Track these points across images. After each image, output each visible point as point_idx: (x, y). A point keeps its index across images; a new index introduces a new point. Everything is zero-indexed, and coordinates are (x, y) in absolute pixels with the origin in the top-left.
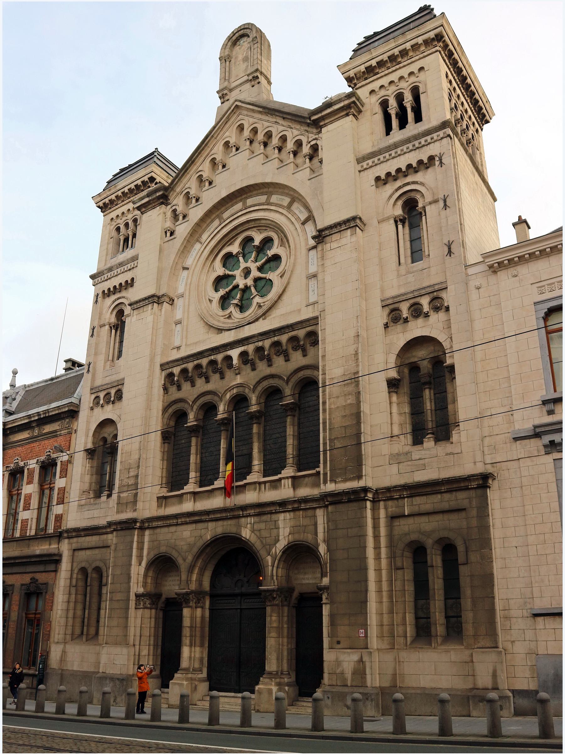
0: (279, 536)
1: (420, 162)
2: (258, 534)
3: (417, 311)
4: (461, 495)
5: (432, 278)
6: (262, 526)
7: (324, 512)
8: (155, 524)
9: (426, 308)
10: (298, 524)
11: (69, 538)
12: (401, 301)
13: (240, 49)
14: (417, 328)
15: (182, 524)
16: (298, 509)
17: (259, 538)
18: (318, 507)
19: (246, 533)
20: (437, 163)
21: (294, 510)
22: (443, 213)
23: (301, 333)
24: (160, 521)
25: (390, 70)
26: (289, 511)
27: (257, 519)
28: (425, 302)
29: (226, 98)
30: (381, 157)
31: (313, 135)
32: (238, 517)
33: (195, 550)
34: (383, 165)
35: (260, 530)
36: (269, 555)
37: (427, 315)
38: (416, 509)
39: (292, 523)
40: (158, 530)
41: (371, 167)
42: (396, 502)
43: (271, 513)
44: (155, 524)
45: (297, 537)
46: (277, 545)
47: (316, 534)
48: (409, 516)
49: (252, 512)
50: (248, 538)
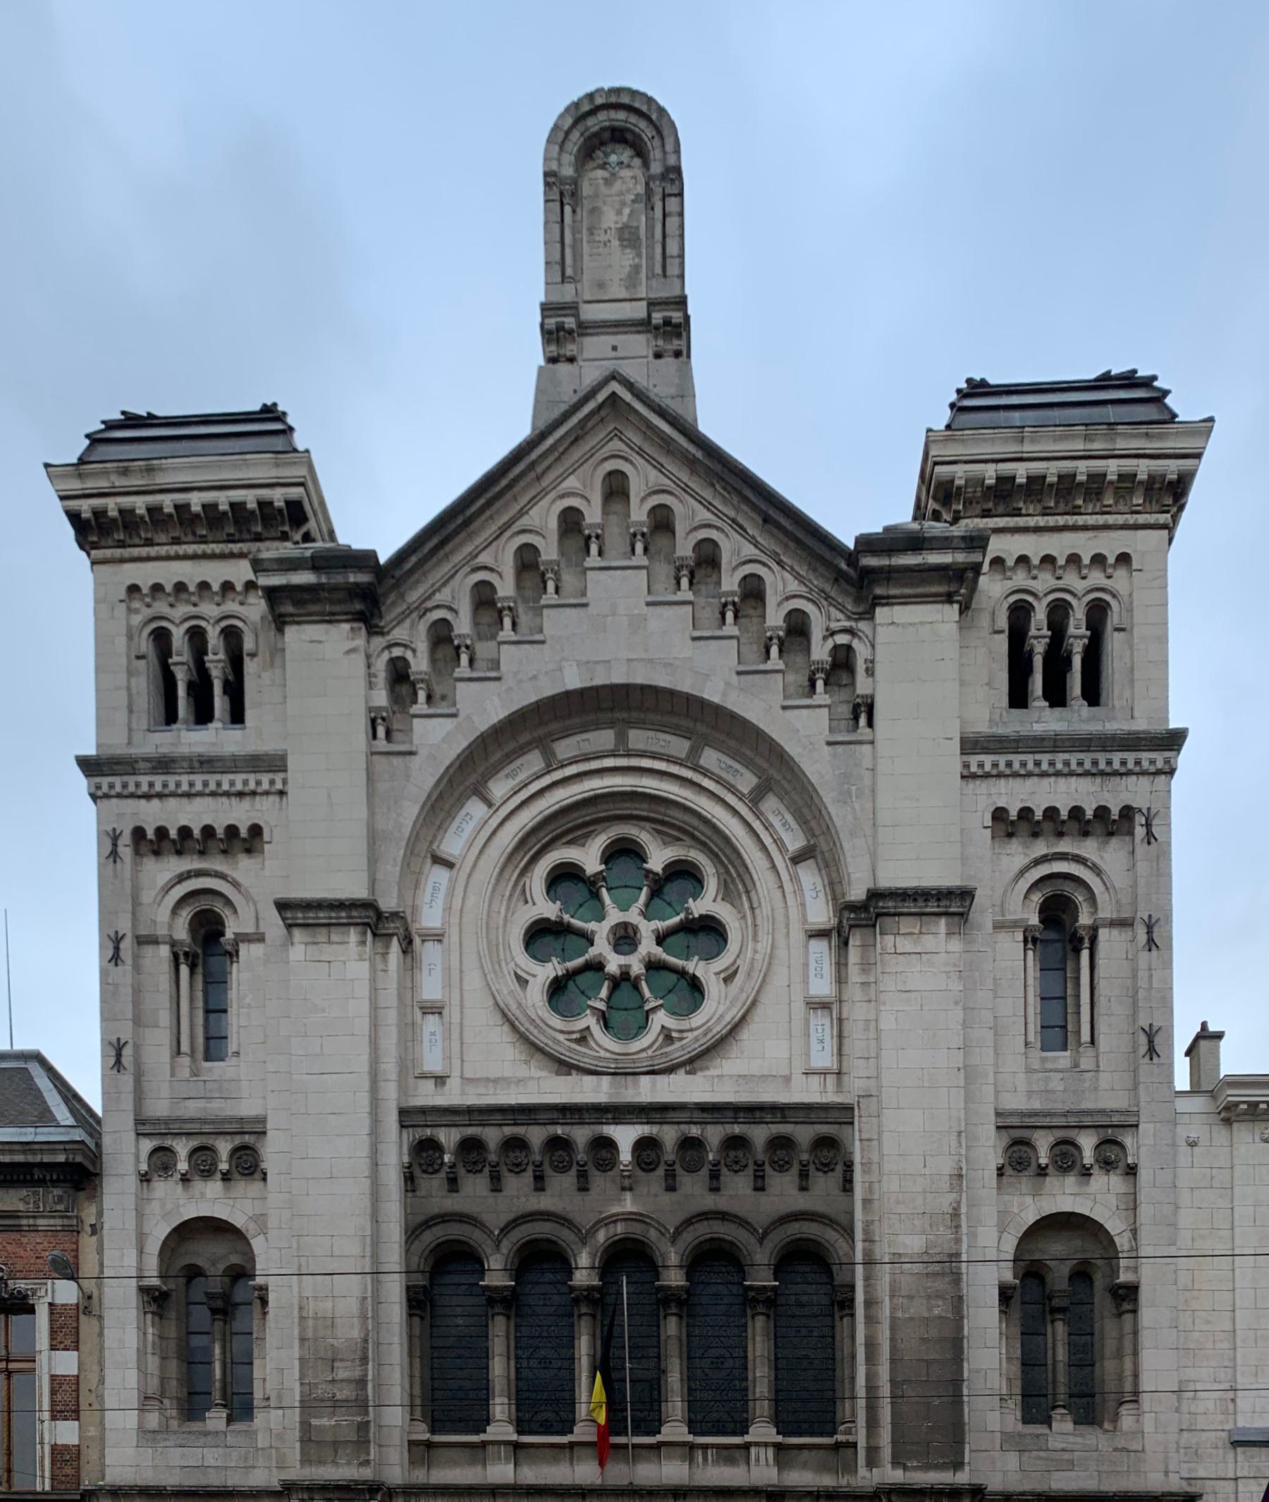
1: (1102, 812)
3: (1066, 1159)
5: (1107, 1094)
9: (1088, 1157)
12: (1036, 1127)
13: (608, 182)
14: (1064, 1196)
20: (1140, 832)
22: (1144, 955)
23: (804, 1134)
25: (1052, 521)
28: (1088, 1143)
29: (570, 349)
30: (1016, 759)
31: (841, 616)
34: (1015, 784)
37: (1086, 1173)
41: (987, 776)
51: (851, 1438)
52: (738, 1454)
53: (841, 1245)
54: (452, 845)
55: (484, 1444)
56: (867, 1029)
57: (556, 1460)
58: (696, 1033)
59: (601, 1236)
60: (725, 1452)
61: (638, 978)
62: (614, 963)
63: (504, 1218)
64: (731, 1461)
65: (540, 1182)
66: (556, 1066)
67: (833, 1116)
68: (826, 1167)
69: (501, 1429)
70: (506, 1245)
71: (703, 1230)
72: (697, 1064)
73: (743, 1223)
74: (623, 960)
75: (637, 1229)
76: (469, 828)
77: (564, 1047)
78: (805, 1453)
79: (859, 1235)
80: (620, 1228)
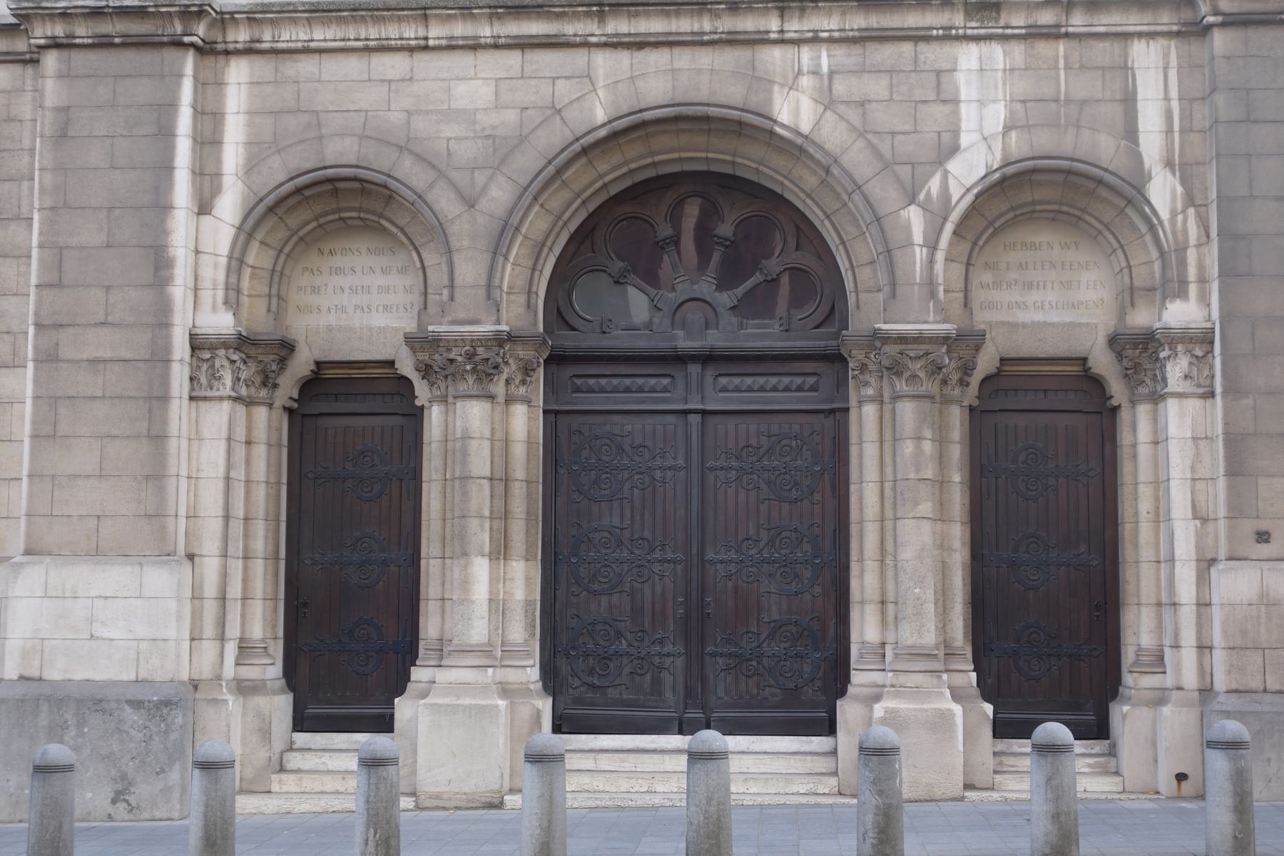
0: (956, 133)
2: (855, 117)
6: (876, 87)
7: (1166, 55)
15: (451, 47)
18: (1140, 35)
19: (794, 110)
24: (326, 22)
26: (1004, 38)
27: (843, 55)
33: (528, 162)
36: (912, 200)
39: (1022, 86)
40: (306, 66)
43: (920, 37)
45: (1045, 142)
46: (953, 166)
47: (1131, 133)
50: (805, 127)
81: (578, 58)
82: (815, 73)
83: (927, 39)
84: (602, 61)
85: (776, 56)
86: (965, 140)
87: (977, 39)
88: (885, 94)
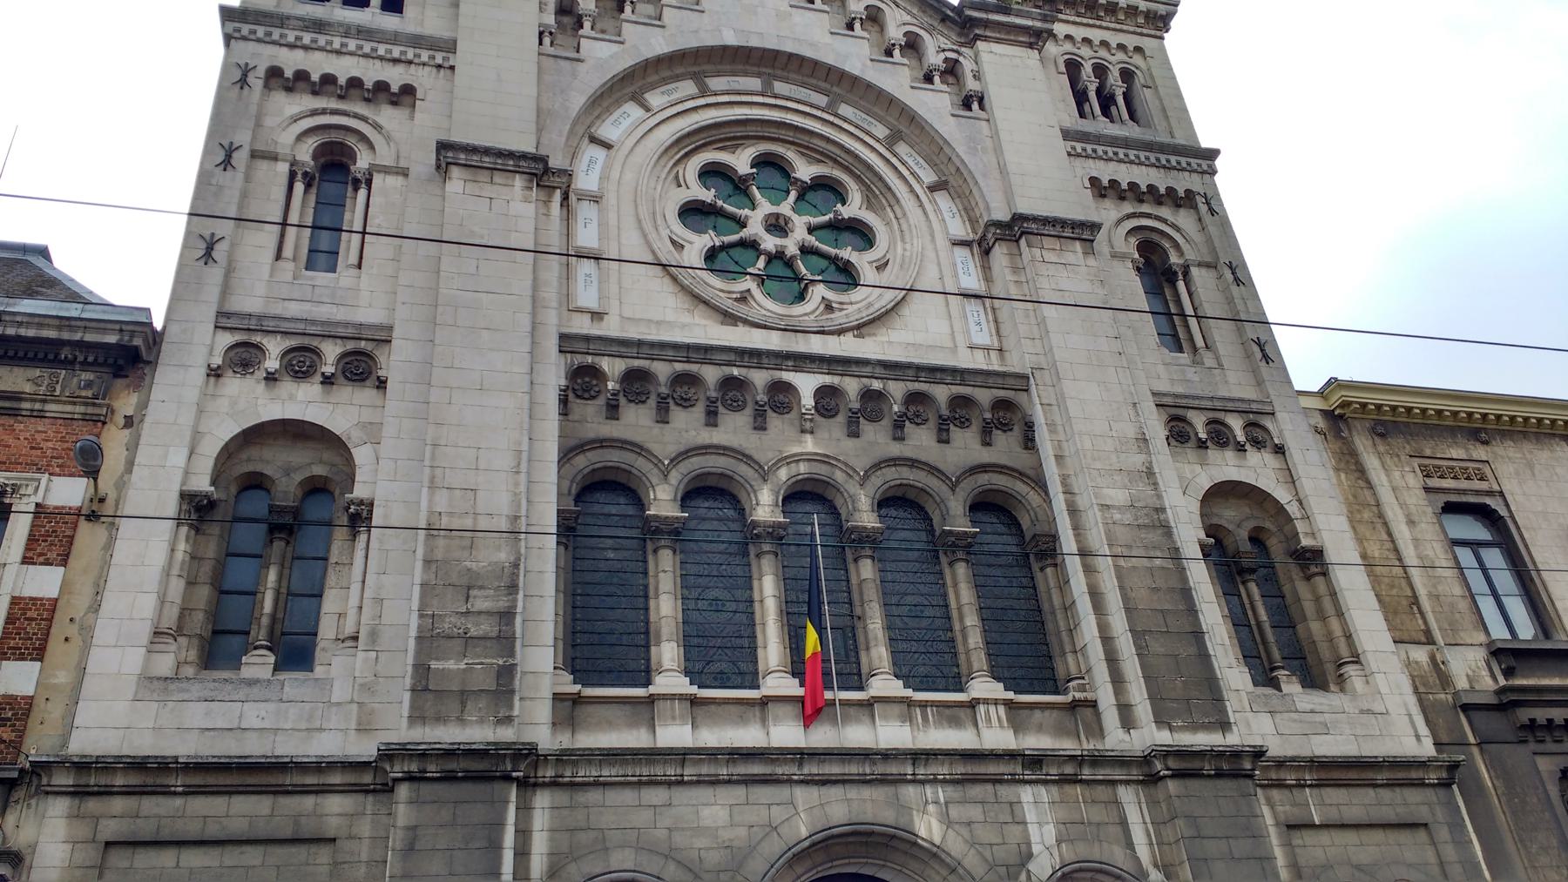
0: (1029, 844)
2: (965, 831)
4: (1413, 796)
6: (975, 813)
7: (1138, 795)
8: (585, 773)
10: (1077, 817)
11: (79, 793)
15: (699, 782)
16: (1073, 780)
17: (973, 843)
19: (928, 828)
21: (1064, 780)
24: (611, 764)
26: (1045, 782)
32: (900, 780)
35: (969, 824)
38: (1333, 815)
39: (1063, 814)
42: (1286, 792)
43: (996, 780)
44: (585, 773)
45: (1083, 851)
47: (1130, 845)
48: (1325, 826)
49: (942, 770)
50: (937, 840)
51: (1089, 696)
52: (962, 713)
53: (1034, 498)
54: (609, 130)
55: (652, 700)
56: (1027, 316)
57: (742, 721)
58: (855, 307)
59: (783, 474)
60: (948, 712)
61: (793, 257)
62: (770, 243)
63: (672, 450)
64: (955, 722)
65: (712, 418)
66: (721, 318)
67: (1011, 382)
68: (1005, 427)
69: (671, 680)
70: (675, 477)
71: (891, 475)
72: (864, 330)
73: (933, 470)
74: (779, 241)
75: (822, 470)
76: (626, 123)
77: (728, 304)
78: (1038, 714)
79: (1055, 488)
80: (803, 468)
81: (782, 792)
82: (936, 802)
83: (1000, 781)
84: (800, 793)
85: (910, 792)
86: (1036, 849)
87: (1030, 782)
88: (981, 818)
